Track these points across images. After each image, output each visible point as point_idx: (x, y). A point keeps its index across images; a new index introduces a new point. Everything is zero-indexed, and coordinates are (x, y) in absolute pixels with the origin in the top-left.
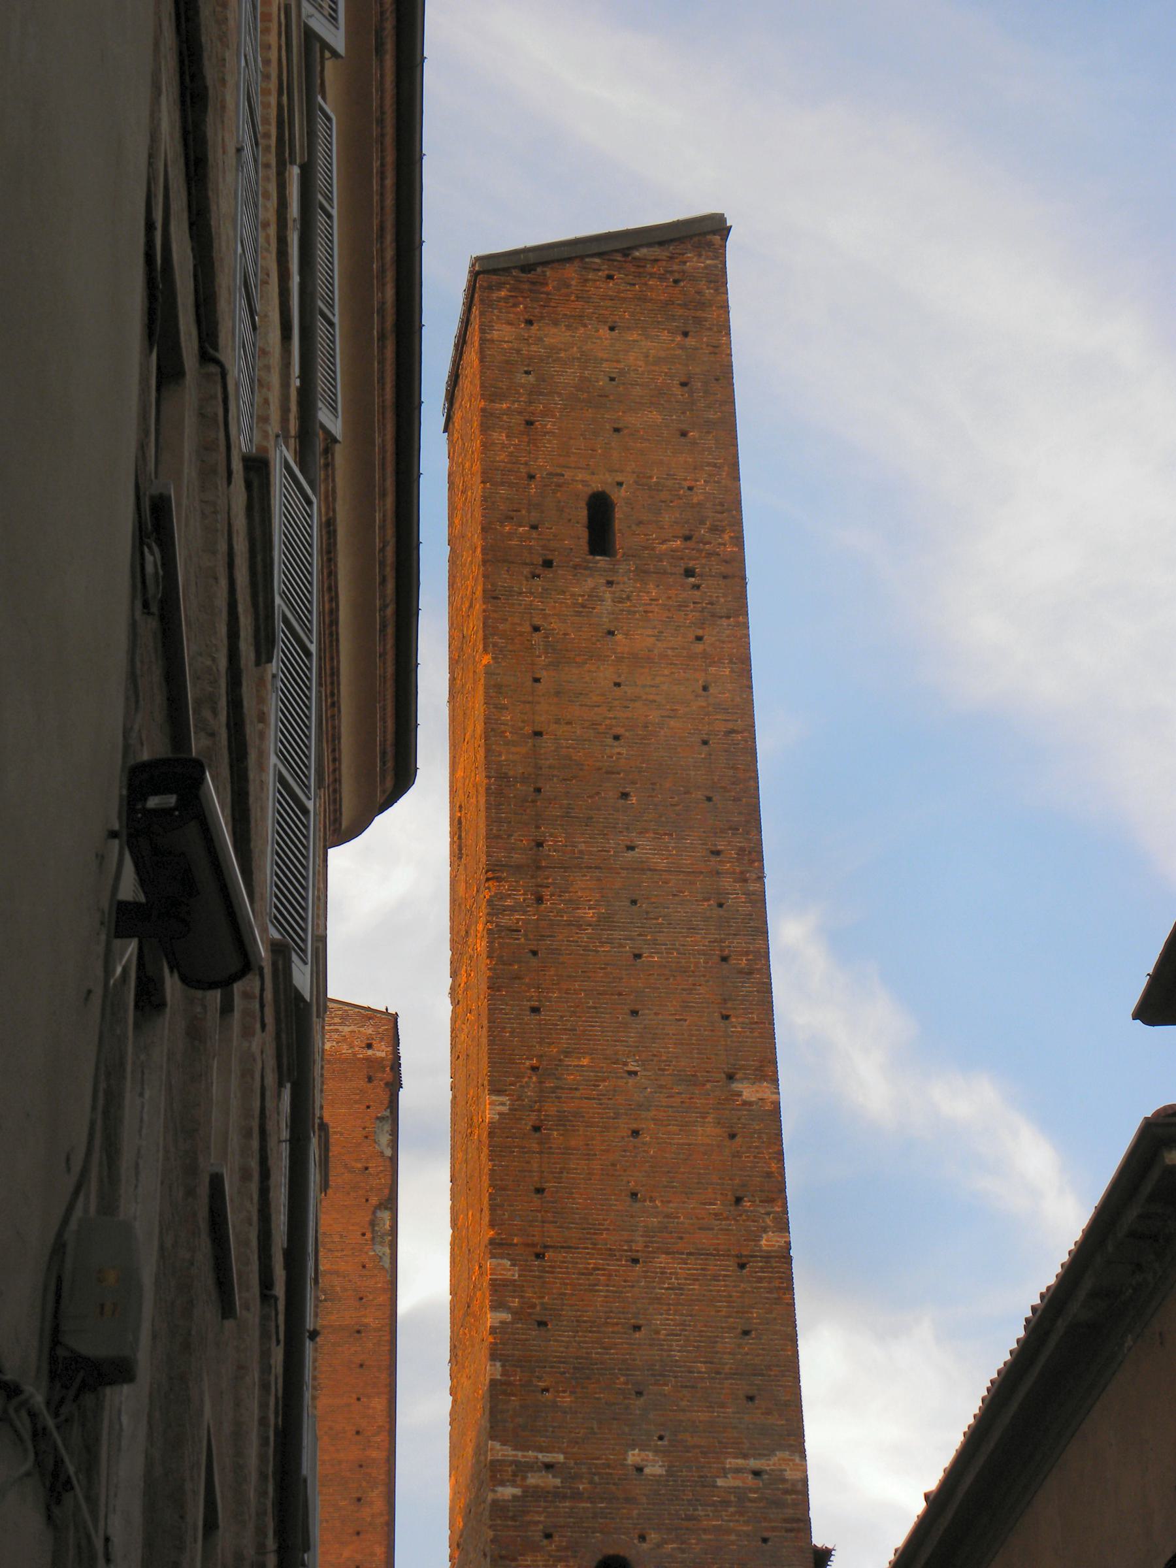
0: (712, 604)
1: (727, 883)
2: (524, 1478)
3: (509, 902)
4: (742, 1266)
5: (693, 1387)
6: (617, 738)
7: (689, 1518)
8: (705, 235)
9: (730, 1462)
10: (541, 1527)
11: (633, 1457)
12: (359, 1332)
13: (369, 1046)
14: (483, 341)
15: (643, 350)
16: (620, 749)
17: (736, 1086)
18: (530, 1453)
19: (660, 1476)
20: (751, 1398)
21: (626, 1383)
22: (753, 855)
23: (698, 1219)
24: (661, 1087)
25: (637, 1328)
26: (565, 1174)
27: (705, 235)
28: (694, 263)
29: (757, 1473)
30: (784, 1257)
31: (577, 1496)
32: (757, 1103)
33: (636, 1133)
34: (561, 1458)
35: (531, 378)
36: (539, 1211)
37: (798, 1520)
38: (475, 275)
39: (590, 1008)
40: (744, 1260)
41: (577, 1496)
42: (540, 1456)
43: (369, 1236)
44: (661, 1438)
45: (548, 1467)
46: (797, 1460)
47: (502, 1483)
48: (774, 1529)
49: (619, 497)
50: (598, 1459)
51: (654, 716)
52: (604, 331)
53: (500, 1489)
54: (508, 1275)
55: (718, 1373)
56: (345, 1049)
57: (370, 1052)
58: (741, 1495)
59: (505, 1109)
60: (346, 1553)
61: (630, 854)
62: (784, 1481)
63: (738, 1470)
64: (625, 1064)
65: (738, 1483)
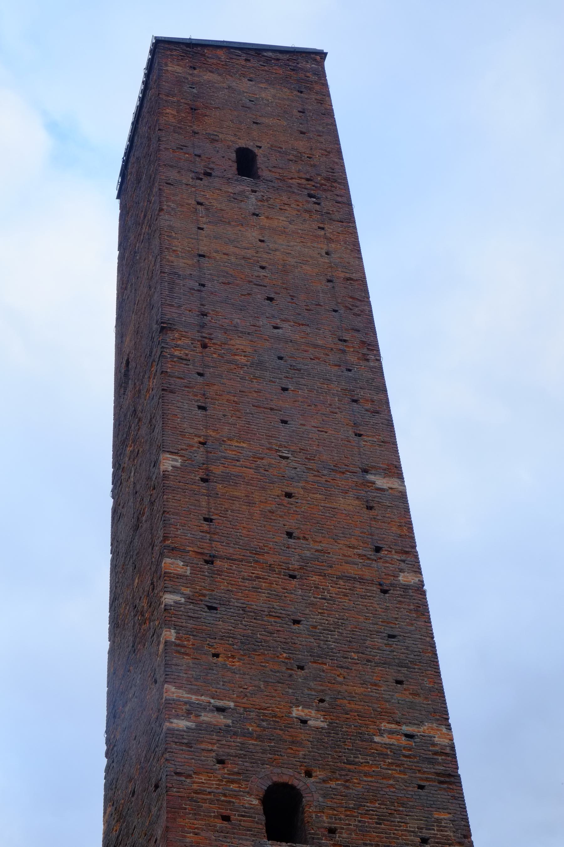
0: (329, 213)
1: (352, 358)
2: (198, 716)
3: (179, 342)
5: (348, 668)
6: (263, 268)
7: (349, 763)
9: (384, 726)
10: (214, 754)
11: (297, 712)
18: (203, 698)
19: (322, 728)
21: (289, 658)
23: (345, 556)
26: (229, 512)
29: (410, 736)
30: (419, 590)
32: (387, 490)
33: (289, 495)
34: (232, 704)
35: (195, 91)
36: (209, 533)
37: (450, 775)
39: (247, 413)
40: (386, 588)
42: (212, 701)
44: (322, 701)
45: (221, 710)
46: (444, 730)
47: (177, 716)
48: (427, 779)
50: (265, 709)
51: (292, 261)
53: (175, 721)
55: (368, 661)
58: (396, 751)
59: (178, 464)
61: (276, 331)
62: (434, 745)
63: (391, 732)
64: (277, 451)
65: (393, 741)
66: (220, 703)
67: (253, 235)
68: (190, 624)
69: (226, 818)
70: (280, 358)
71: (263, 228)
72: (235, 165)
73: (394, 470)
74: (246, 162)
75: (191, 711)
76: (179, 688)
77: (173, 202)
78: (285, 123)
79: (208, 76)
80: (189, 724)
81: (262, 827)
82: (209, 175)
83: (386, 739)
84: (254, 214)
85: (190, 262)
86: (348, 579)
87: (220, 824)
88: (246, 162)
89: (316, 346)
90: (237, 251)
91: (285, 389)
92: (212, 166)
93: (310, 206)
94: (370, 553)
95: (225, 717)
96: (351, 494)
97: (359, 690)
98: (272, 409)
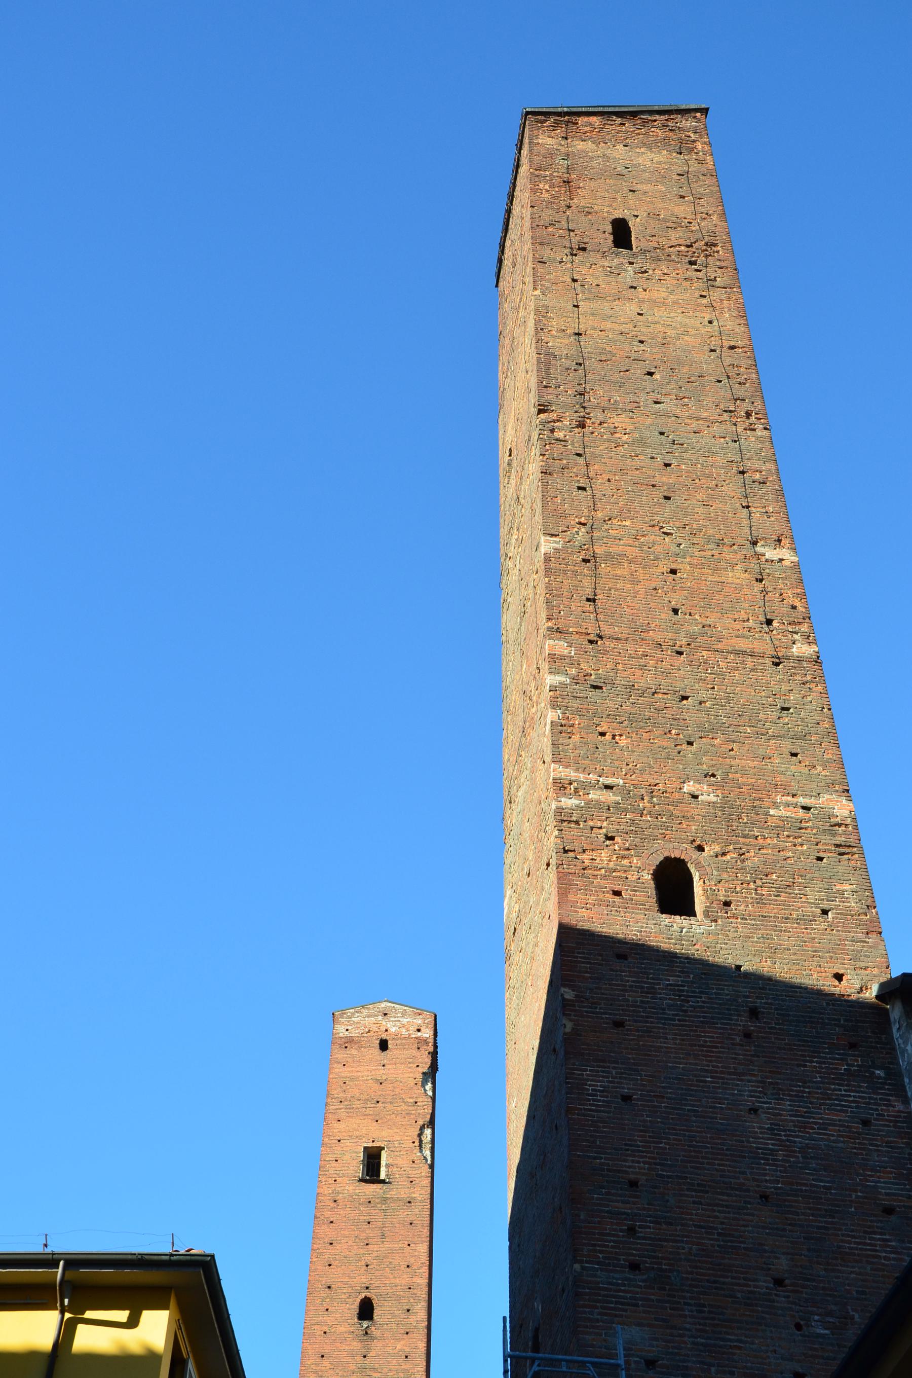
4: (777, 664)
6: (642, 342)
10: (604, 830)
12: (409, 1202)
13: (419, 1030)
14: (530, 143)
20: (795, 755)
24: (693, 544)
25: (685, 698)
26: (613, 592)
29: (806, 808)
33: (673, 572)
43: (417, 1143)
45: (608, 787)
52: (620, 147)
54: (566, 652)
56: (404, 1033)
57: (419, 1034)
59: (559, 546)
60: (399, 1347)
61: (658, 405)
63: (788, 805)
64: (662, 527)
66: (610, 781)
67: (631, 309)
68: (575, 704)
69: (617, 893)
70: (662, 433)
71: (642, 301)
72: (611, 237)
74: (621, 234)
76: (567, 767)
77: (549, 280)
78: (664, 189)
79: (580, 145)
80: (577, 802)
81: (653, 901)
82: (584, 249)
83: (782, 812)
84: (632, 287)
85: (566, 341)
86: (737, 653)
87: (610, 898)
88: (621, 234)
89: (699, 419)
90: (616, 327)
91: (667, 465)
92: (585, 240)
93: (690, 274)
95: (614, 794)
96: (738, 567)
97: (751, 764)
98: (653, 486)
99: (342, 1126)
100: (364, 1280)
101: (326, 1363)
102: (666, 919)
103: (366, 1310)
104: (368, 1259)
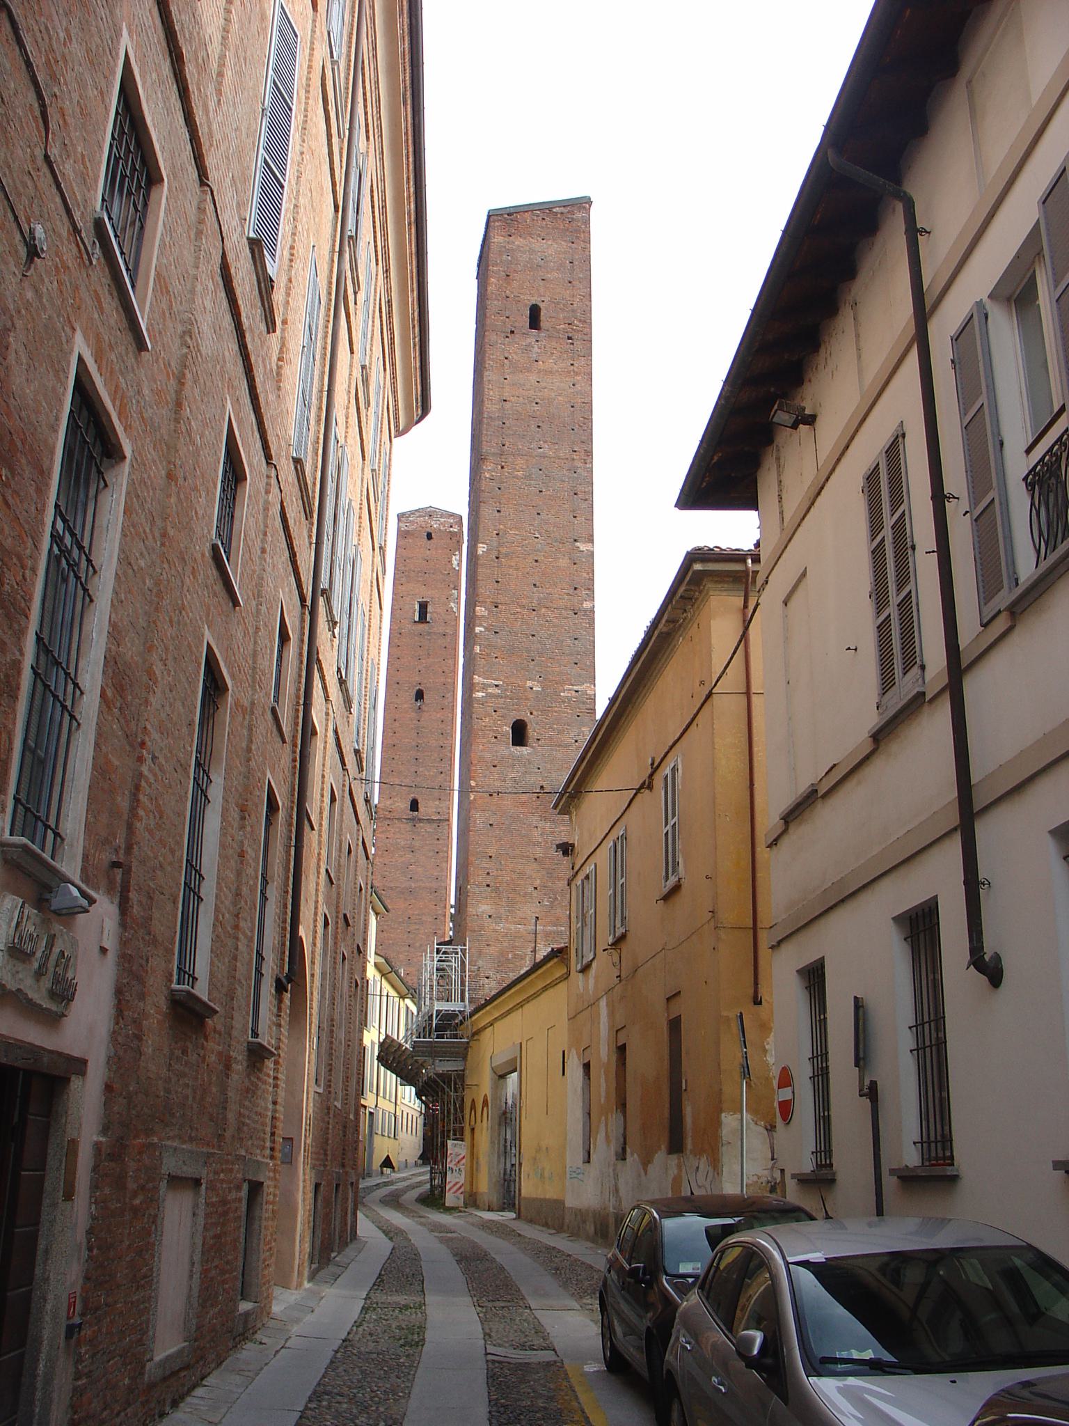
8: (583, 204)
9: (567, 687)
11: (529, 683)
15: (552, 248)
16: (537, 408)
17: (577, 544)
22: (589, 453)
27: (583, 204)
28: (578, 215)
31: (507, 697)
38: (489, 216)
41: (507, 697)
49: (541, 305)
58: (570, 699)
67: (533, 378)
73: (590, 539)
75: (484, 687)
77: (493, 360)
87: (494, 740)
94: (571, 591)
99: (403, 588)
100: (418, 679)
101: (397, 724)
102: (513, 749)
103: (420, 695)
104: (420, 667)
